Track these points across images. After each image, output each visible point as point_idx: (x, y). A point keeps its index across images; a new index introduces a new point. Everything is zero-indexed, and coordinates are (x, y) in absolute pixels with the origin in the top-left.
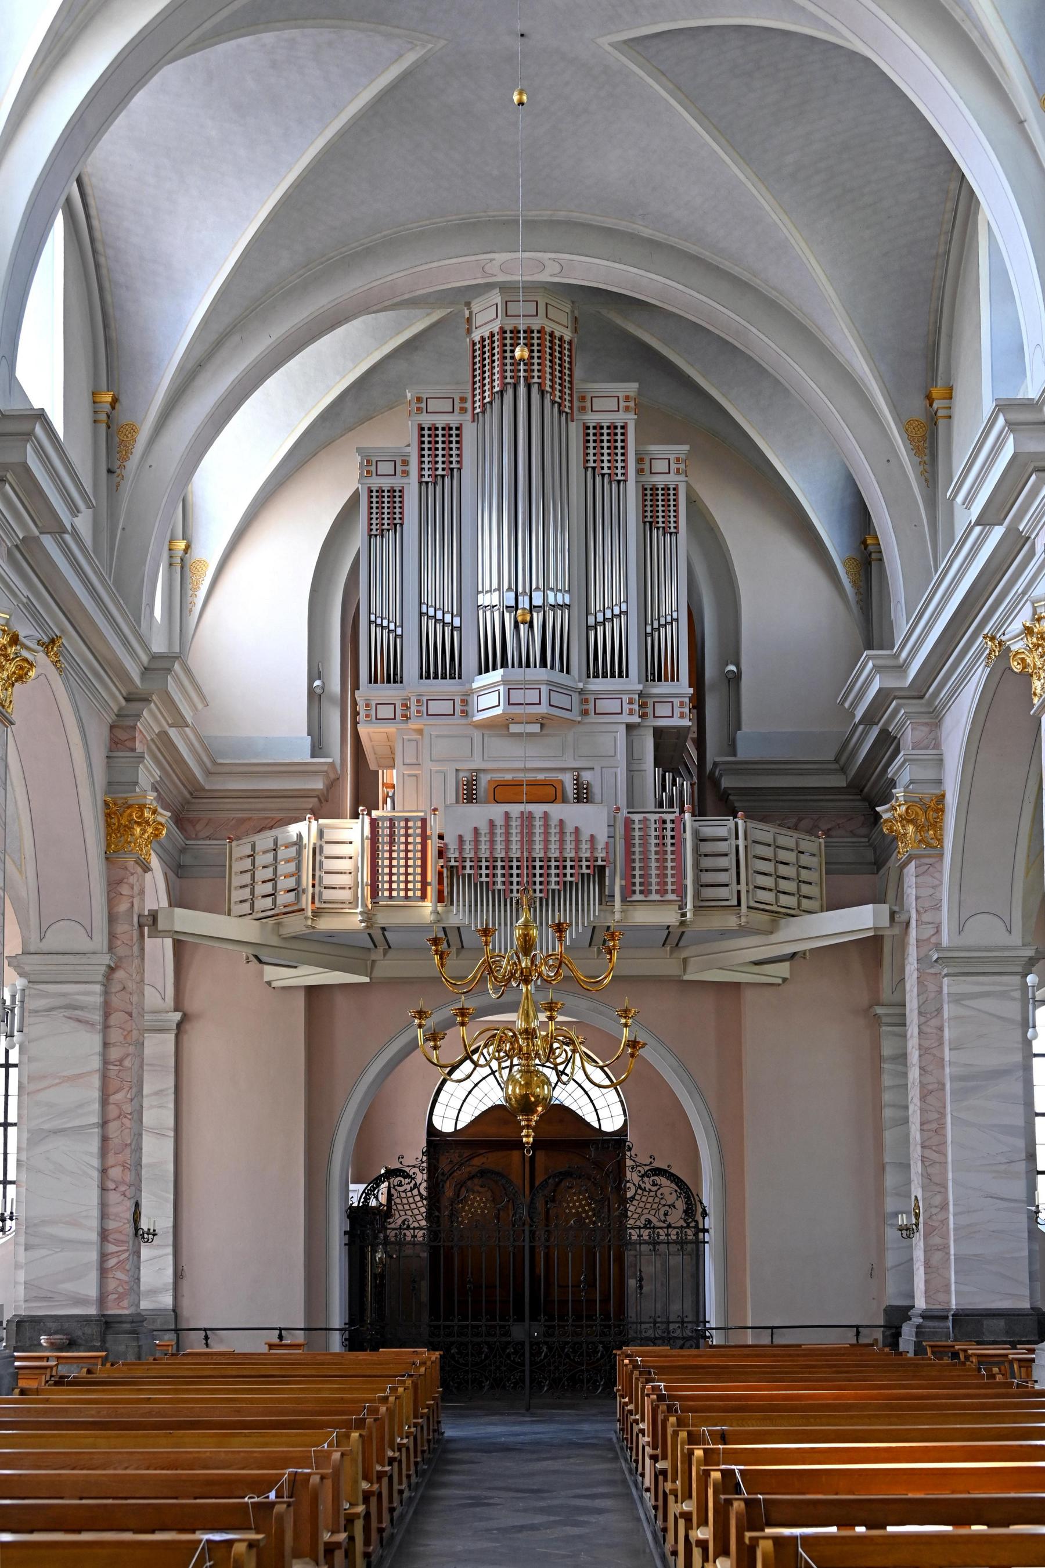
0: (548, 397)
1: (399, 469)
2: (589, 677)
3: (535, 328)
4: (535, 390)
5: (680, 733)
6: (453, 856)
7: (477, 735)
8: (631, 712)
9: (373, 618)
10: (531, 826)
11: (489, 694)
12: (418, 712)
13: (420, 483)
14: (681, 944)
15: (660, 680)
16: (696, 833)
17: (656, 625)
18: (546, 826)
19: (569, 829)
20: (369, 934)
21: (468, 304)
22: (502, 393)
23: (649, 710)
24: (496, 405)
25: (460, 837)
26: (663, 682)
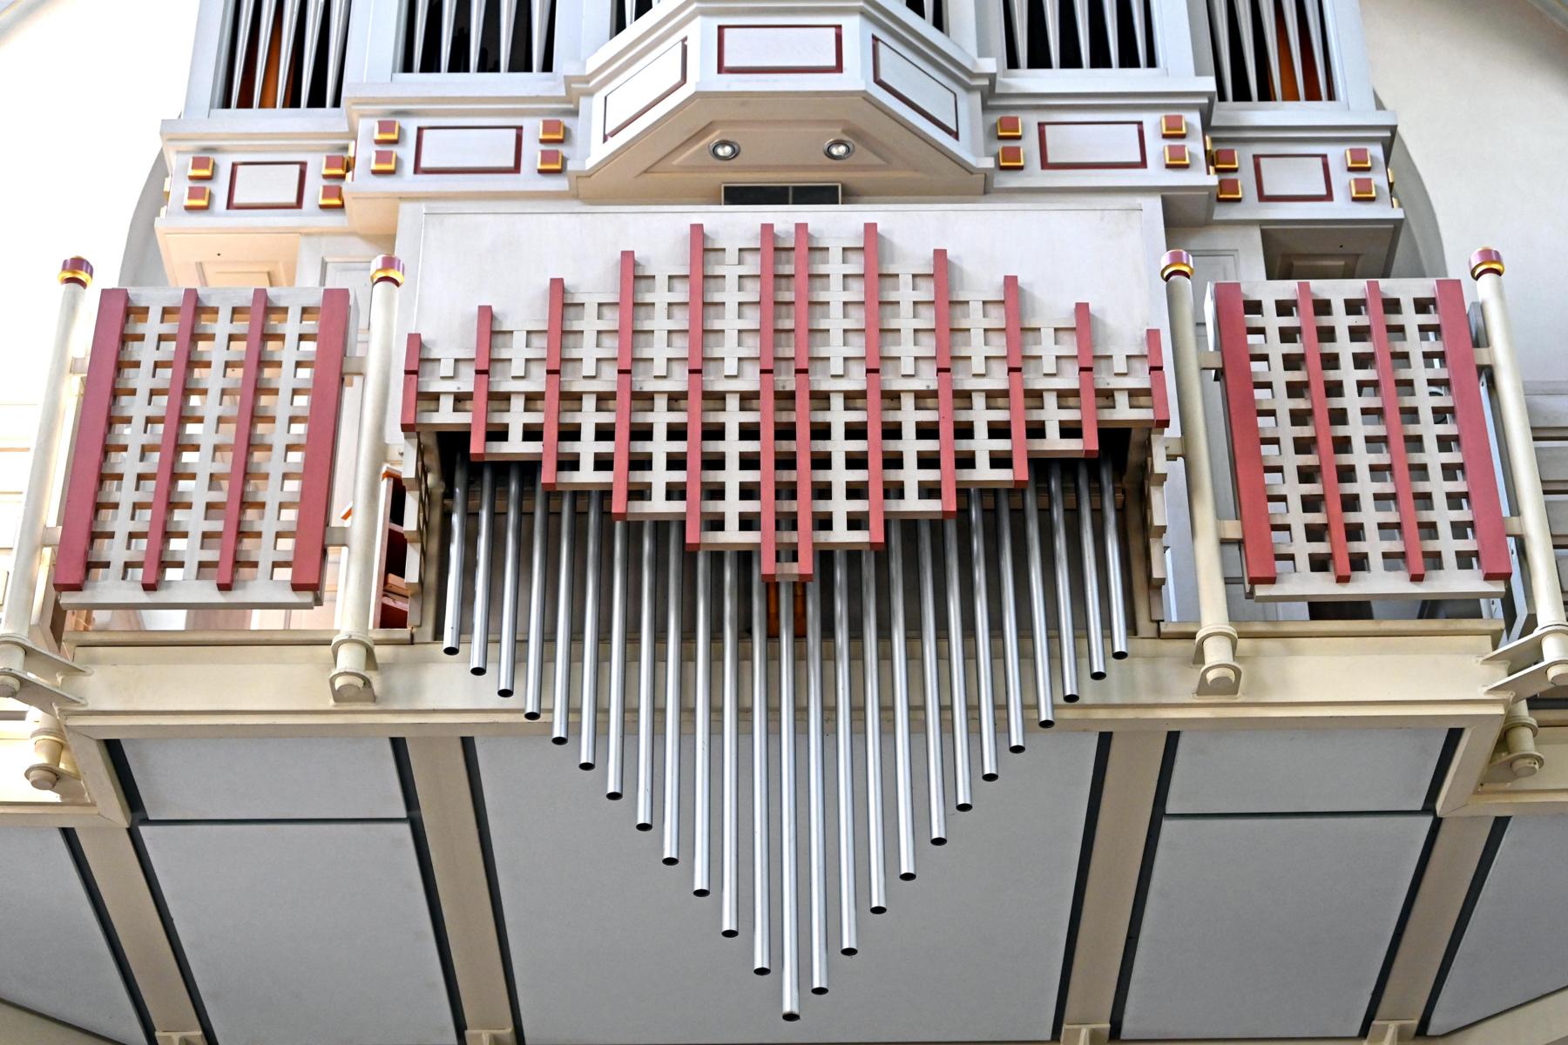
6: (452, 386)
14: (1437, 1024)
20: (69, 835)
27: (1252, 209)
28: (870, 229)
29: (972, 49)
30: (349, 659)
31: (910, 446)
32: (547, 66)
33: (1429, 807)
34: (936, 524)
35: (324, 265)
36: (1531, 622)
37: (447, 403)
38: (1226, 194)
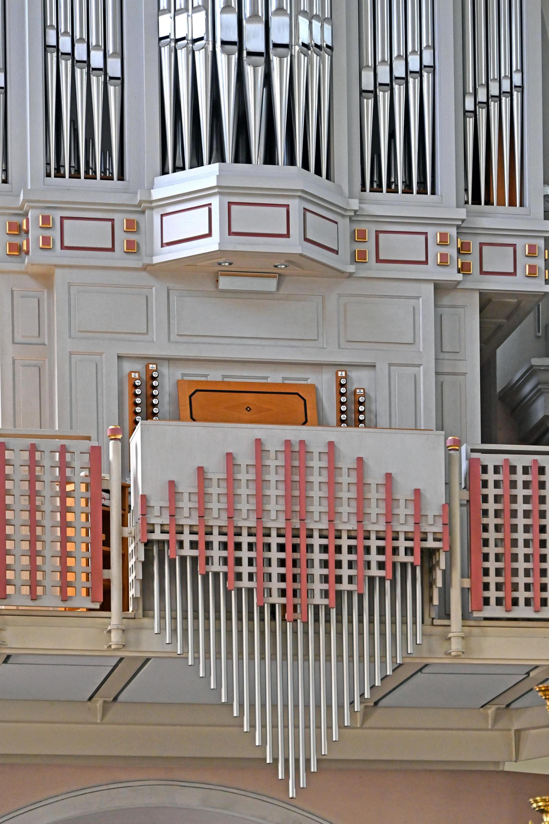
2: (363, 189)
7: (157, 290)
8: (444, 262)
10: (305, 469)
11: (191, 211)
12: (46, 240)
15: (488, 202)
17: (482, 97)
18: (332, 469)
19: (374, 478)
23: (473, 259)
25: (172, 484)
26: (495, 207)
35: (12, 292)
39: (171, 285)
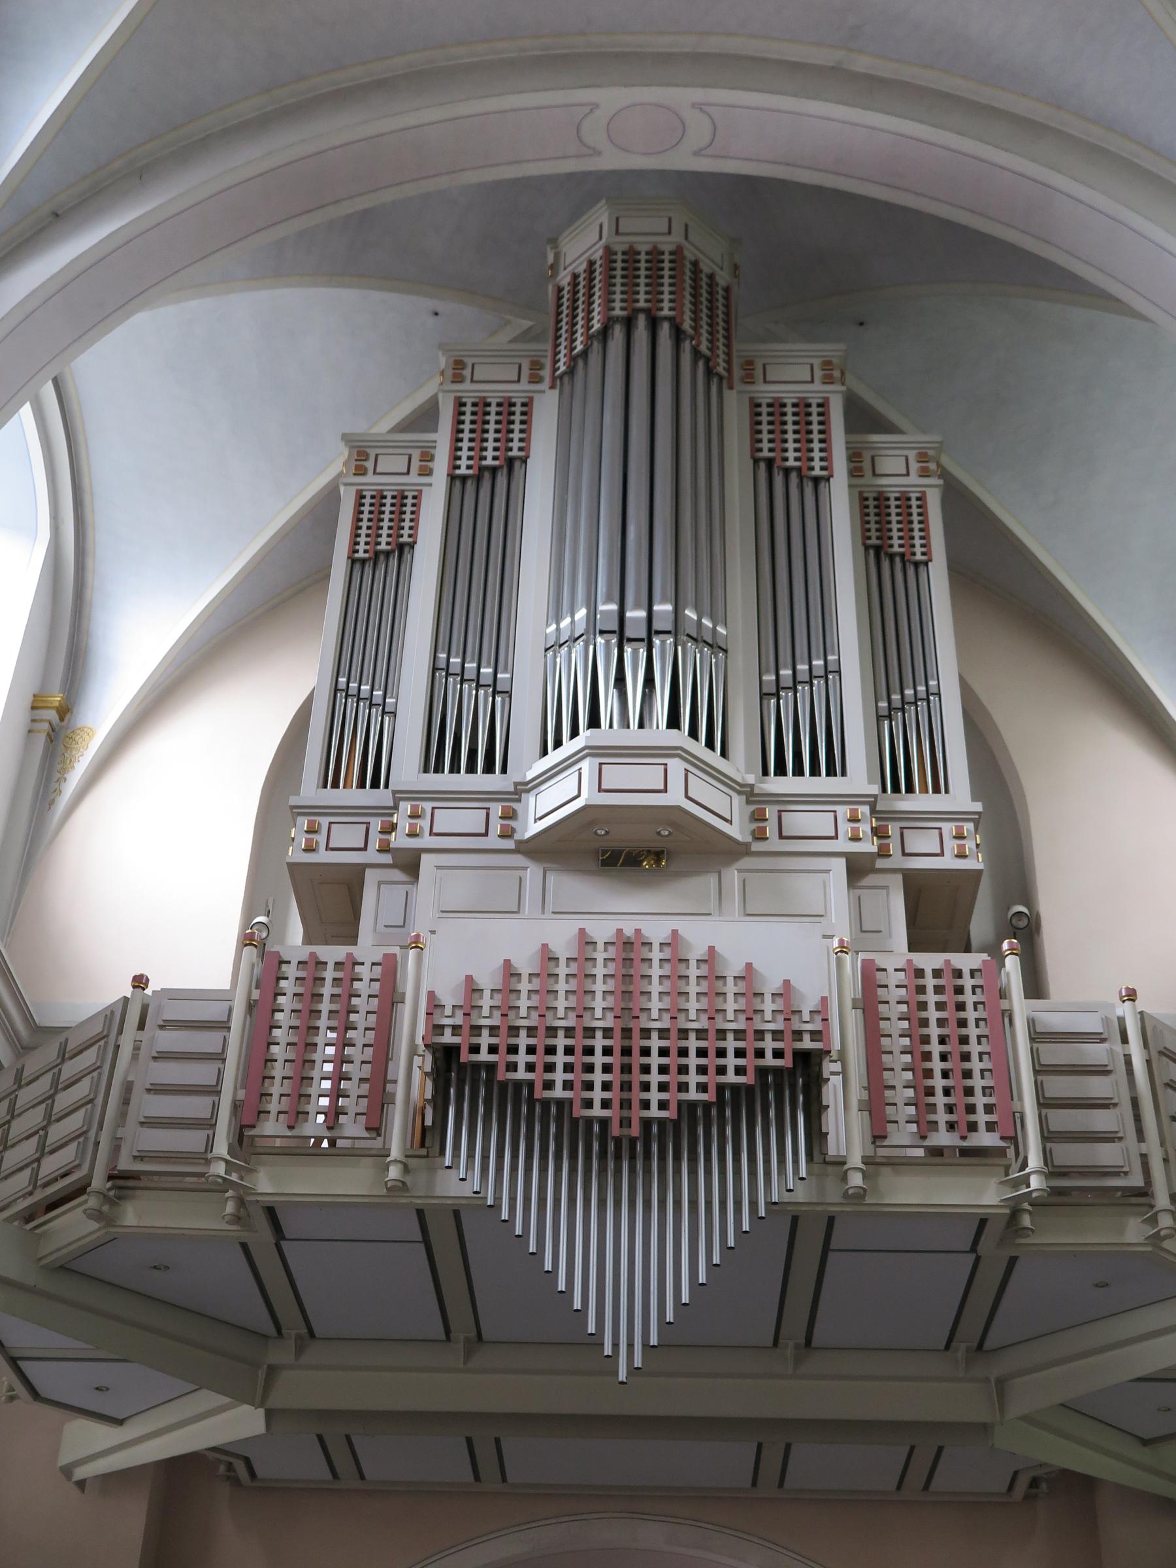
0: (687, 346)
1: (416, 464)
3: (667, 248)
4: (665, 330)
5: (960, 885)
7: (532, 873)
9: (342, 680)
13: (452, 478)
14: (989, 1344)
16: (1031, 1023)
20: (244, 1246)
21: (554, 242)
22: (605, 333)
24: (595, 357)
27: (897, 861)
28: (675, 933)
29: (742, 768)
30: (394, 1172)
31: (693, 1061)
32: (504, 770)
33: (974, 1248)
34: (707, 1106)
36: (1024, 1165)
37: (448, 1031)
38: (883, 853)
39: (547, 865)
